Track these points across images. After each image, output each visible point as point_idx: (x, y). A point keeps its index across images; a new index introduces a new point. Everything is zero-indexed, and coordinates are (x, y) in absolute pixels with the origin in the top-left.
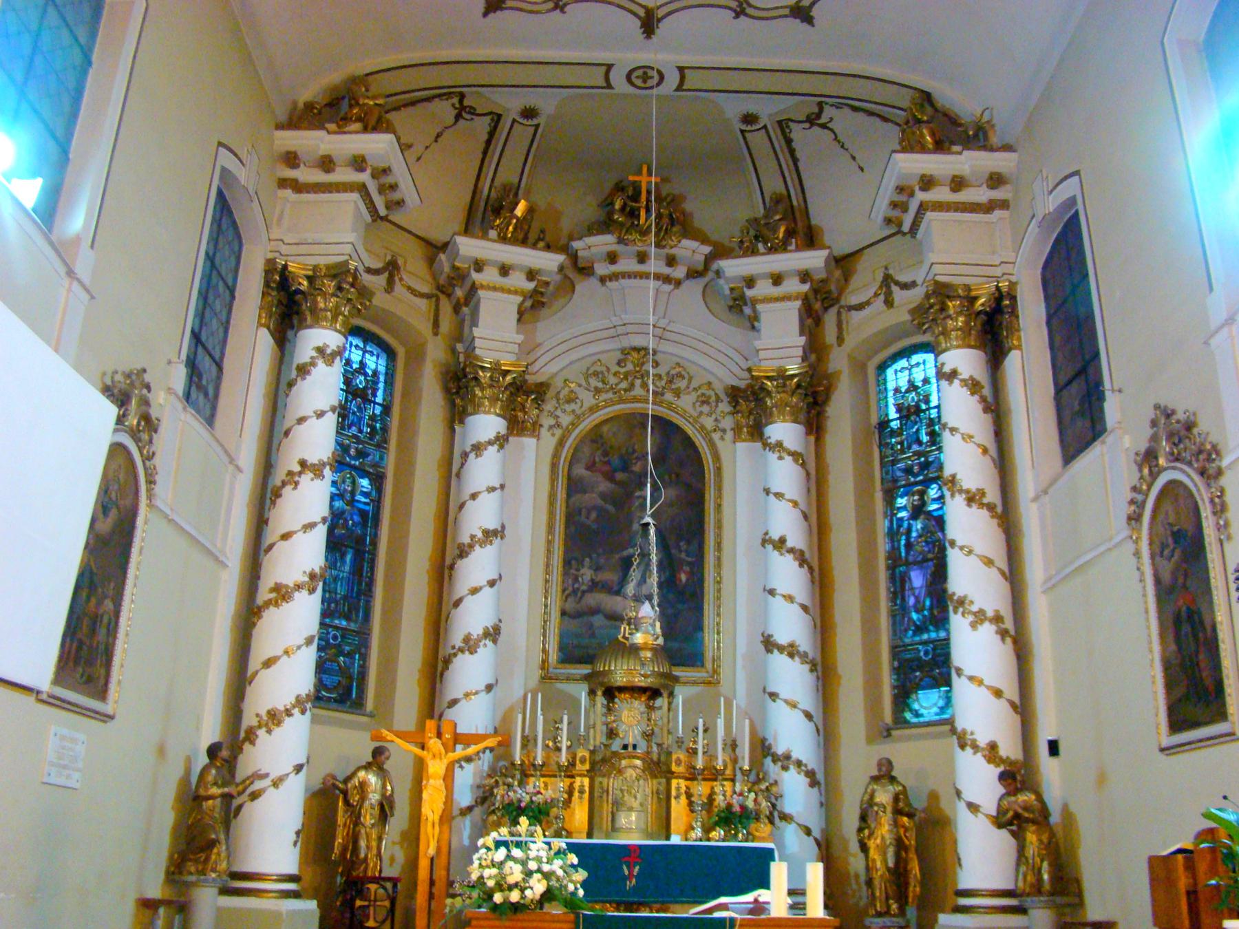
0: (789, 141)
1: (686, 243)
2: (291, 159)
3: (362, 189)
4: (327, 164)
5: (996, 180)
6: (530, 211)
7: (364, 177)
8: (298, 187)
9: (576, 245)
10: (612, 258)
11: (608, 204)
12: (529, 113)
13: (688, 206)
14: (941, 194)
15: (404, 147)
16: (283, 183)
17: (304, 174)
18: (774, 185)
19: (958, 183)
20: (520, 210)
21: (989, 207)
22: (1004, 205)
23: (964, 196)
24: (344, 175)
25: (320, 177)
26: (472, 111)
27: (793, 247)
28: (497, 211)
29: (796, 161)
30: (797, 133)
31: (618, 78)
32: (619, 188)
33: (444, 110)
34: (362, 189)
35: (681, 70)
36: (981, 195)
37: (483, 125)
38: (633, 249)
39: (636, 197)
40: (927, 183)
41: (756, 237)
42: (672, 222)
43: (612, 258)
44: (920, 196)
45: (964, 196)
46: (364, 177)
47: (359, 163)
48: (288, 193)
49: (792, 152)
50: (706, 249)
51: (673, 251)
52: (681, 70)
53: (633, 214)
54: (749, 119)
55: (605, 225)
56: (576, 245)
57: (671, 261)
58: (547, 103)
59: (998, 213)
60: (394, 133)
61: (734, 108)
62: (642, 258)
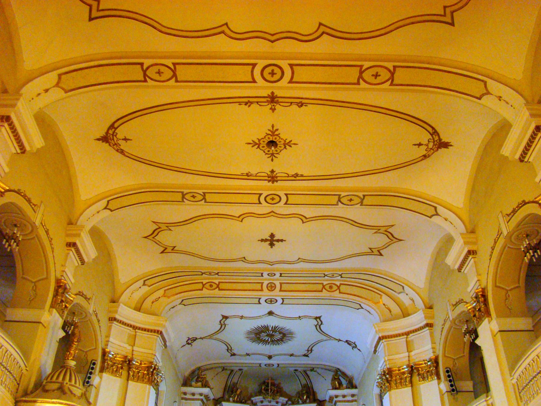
0: (307, 374)
1: (281, 398)
2: (185, 394)
3: (202, 400)
4: (193, 394)
5: (353, 396)
6: (241, 392)
7: (202, 397)
8: (186, 399)
9: (252, 399)
10: (262, 402)
11: (260, 385)
12: (240, 370)
13: (282, 385)
14: (340, 398)
15: (211, 389)
16: (182, 399)
17: (188, 396)
18: (304, 382)
19: (344, 396)
20: (238, 392)
21: (352, 401)
22: (356, 401)
23: (346, 399)
24: (197, 396)
25: (192, 397)
26: (226, 369)
27: (308, 401)
28: (232, 392)
29: (309, 377)
30: (308, 372)
31: (263, 366)
32: (264, 383)
33: (220, 370)
34: (202, 400)
35: (278, 364)
36: (350, 398)
37: (229, 372)
38: (267, 399)
39: (268, 386)
40: (337, 396)
41: (299, 397)
42: (277, 392)
43: (262, 402)
44: (335, 399)
45: (346, 399)
46: (202, 397)
47: (201, 394)
48: (184, 401)
49: (308, 375)
50: (286, 399)
51: (278, 400)
52: (278, 364)
53: (267, 390)
54: (296, 370)
55: (260, 393)
56: (252, 399)
57: (277, 402)
58: (245, 369)
59: (354, 403)
60: (209, 387)
61: (292, 369)
62: (270, 402)
